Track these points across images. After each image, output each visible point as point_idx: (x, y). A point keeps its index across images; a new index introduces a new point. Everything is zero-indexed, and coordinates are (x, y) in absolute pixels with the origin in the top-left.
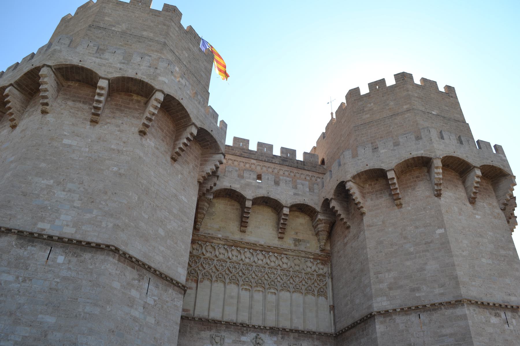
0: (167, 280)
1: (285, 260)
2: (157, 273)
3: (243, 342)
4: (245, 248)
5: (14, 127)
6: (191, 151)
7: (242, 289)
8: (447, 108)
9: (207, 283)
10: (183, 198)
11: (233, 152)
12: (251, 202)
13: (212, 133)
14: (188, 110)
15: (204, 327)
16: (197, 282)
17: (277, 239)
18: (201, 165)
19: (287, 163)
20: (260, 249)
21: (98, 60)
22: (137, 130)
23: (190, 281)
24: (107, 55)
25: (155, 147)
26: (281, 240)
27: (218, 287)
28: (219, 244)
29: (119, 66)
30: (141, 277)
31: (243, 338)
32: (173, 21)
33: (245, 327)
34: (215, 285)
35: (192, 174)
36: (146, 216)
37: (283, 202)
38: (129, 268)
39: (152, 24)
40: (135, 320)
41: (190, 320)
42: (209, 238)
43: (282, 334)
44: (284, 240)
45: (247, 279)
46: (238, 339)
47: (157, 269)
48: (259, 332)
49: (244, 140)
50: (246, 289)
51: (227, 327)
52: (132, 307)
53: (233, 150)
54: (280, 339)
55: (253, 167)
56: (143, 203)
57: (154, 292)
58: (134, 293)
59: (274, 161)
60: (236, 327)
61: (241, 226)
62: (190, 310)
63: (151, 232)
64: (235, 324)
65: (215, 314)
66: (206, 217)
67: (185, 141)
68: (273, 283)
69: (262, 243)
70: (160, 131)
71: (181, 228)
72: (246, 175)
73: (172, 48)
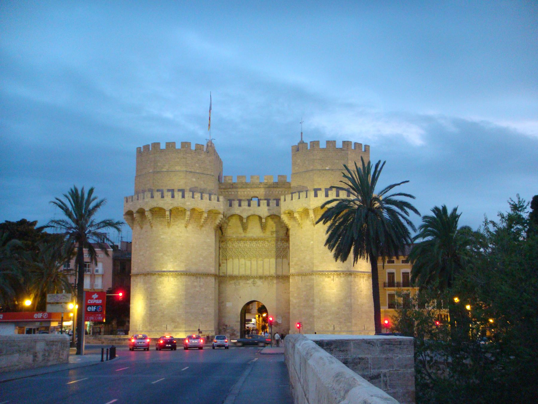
1: (267, 243)
5: (142, 228)
8: (337, 161)
9: (231, 259)
16: (226, 260)
18: (215, 220)
21: (163, 202)
22: (183, 225)
24: (165, 198)
27: (236, 261)
29: (171, 202)
30: (197, 278)
31: (248, 282)
37: (262, 216)
39: (178, 160)
40: (198, 291)
55: (249, 193)
57: (203, 280)
58: (196, 284)
64: (244, 277)
65: (236, 273)
69: (255, 236)
72: (243, 203)
73: (190, 170)
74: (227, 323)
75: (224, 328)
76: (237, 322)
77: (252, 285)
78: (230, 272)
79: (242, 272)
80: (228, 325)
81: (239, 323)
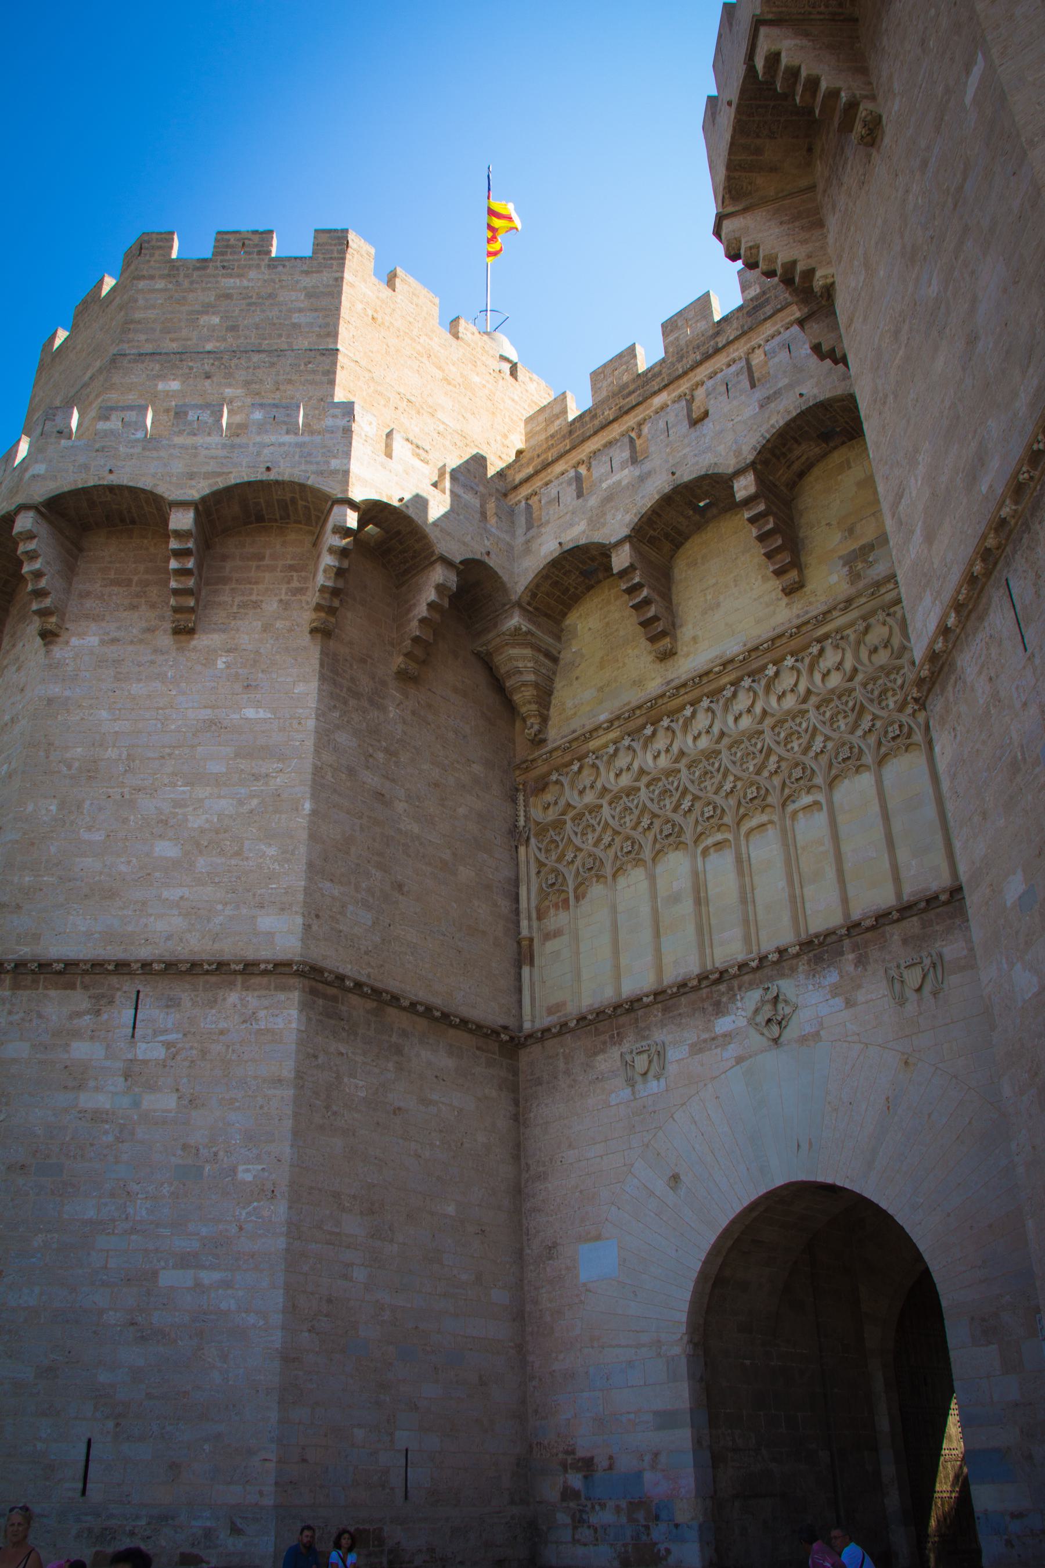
0: (207, 972)
2: (156, 966)
3: (725, 1035)
4: (683, 708)
6: (266, 562)
7: (705, 852)
9: (596, 890)
10: (250, 713)
11: (596, 422)
12: (627, 547)
13: (272, 476)
14: (145, 483)
15: (602, 1038)
17: (785, 600)
19: (768, 310)
20: (733, 677)
23: (552, 911)
25: (102, 642)
26: (796, 596)
27: (633, 885)
28: (606, 746)
30: (102, 1001)
31: (723, 1024)
32: (143, 277)
33: (718, 981)
34: (622, 881)
35: (279, 624)
36: (98, 837)
38: (53, 993)
40: (98, 1117)
41: (560, 1034)
42: (575, 745)
43: (855, 947)
44: (808, 589)
45: (709, 811)
46: (705, 1036)
47: (150, 958)
48: (771, 979)
49: (620, 356)
50: (717, 844)
51: (666, 1010)
52: (80, 1087)
53: (595, 416)
54: (850, 968)
56: (79, 807)
59: (721, 341)
60: (693, 996)
61: (653, 639)
62: (564, 1004)
63: (123, 868)
64: (683, 987)
66: (558, 684)
67: (173, 564)
68: (798, 773)
70: (116, 589)
71: (255, 802)
73: (149, 348)
74: (586, 1442)
75: (568, 1494)
76: (665, 1420)
77: (756, 1040)
78: (594, 990)
79: (682, 961)
80: (601, 1462)
81: (683, 1437)
